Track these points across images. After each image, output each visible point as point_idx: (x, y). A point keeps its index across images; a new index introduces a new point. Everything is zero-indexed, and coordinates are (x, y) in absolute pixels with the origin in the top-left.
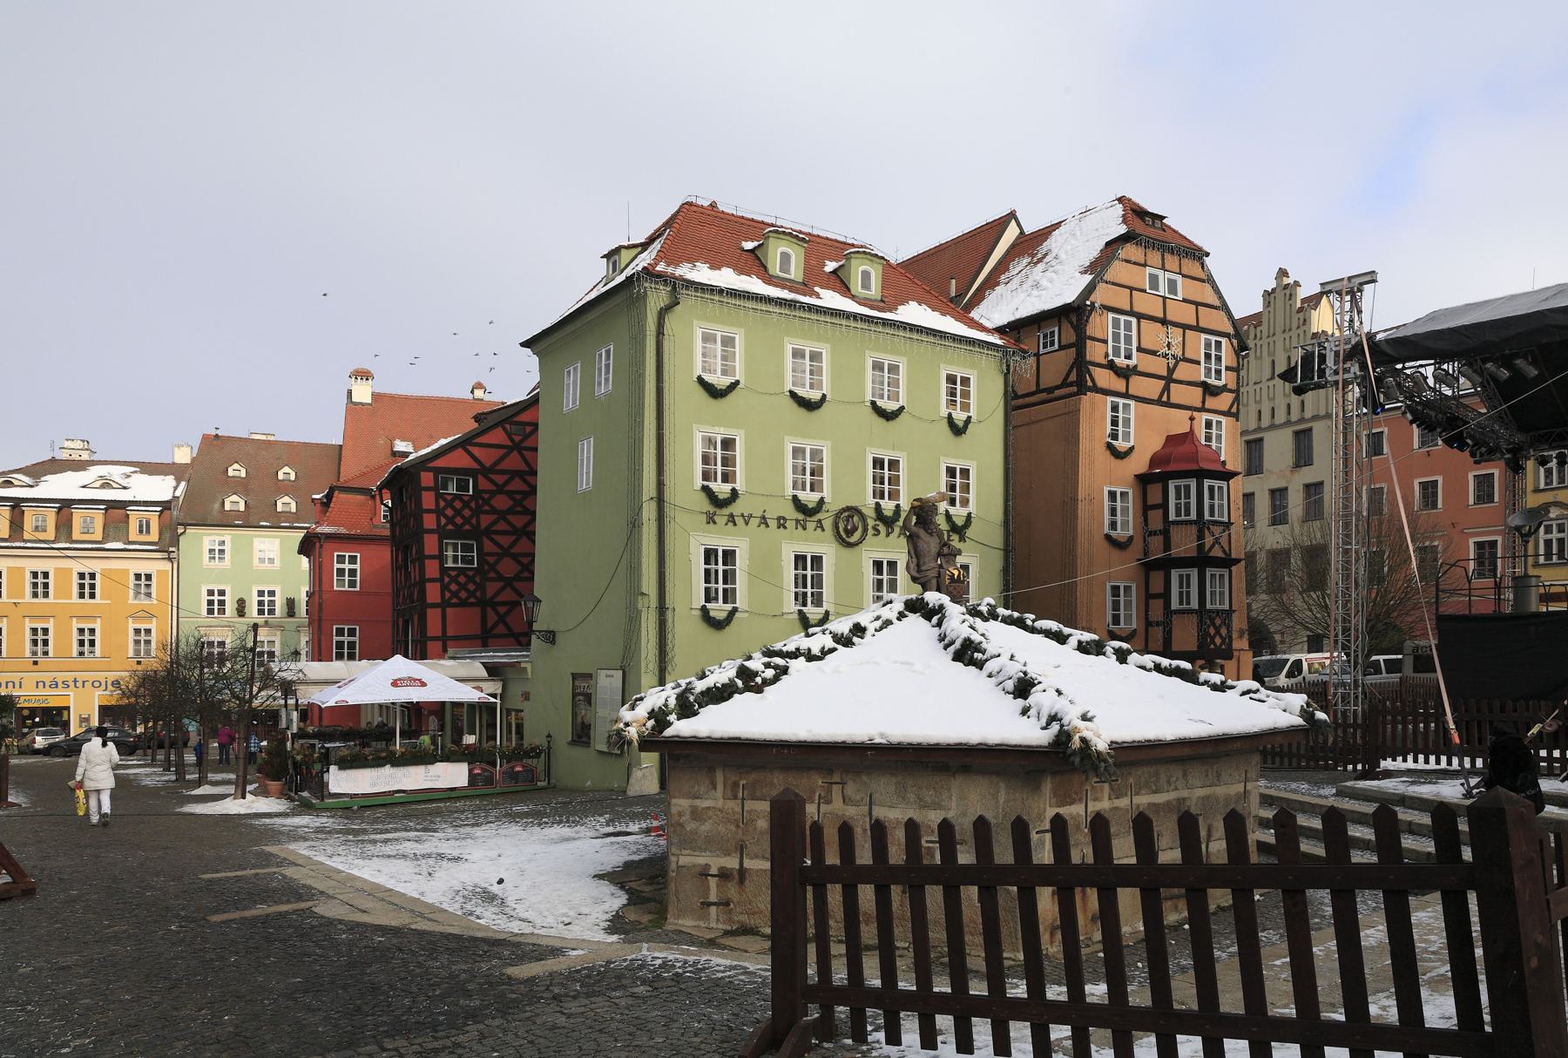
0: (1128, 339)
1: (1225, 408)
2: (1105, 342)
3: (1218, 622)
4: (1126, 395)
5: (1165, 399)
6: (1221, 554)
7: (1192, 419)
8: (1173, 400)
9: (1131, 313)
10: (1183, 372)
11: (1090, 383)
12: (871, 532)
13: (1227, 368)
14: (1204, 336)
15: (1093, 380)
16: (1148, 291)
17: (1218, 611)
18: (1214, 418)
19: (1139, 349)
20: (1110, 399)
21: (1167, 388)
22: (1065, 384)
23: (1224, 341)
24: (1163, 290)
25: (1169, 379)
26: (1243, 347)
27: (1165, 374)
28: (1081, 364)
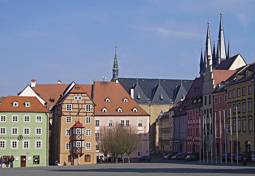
0: (70, 108)
1: (91, 115)
2: (66, 108)
3: (79, 149)
4: (70, 116)
5: (78, 115)
6: (80, 139)
7: (79, 119)
8: (79, 115)
9: (71, 103)
10: (81, 111)
11: (63, 115)
12: (23, 138)
13: (91, 109)
14: (86, 105)
15: (63, 114)
16: (75, 99)
17: (78, 148)
18: (88, 117)
19: (72, 109)
20: (67, 116)
21: (78, 114)
22: (60, 115)
23: (91, 105)
24: (78, 99)
25: (79, 112)
26: (95, 105)
27: (78, 111)
28: (62, 112)
